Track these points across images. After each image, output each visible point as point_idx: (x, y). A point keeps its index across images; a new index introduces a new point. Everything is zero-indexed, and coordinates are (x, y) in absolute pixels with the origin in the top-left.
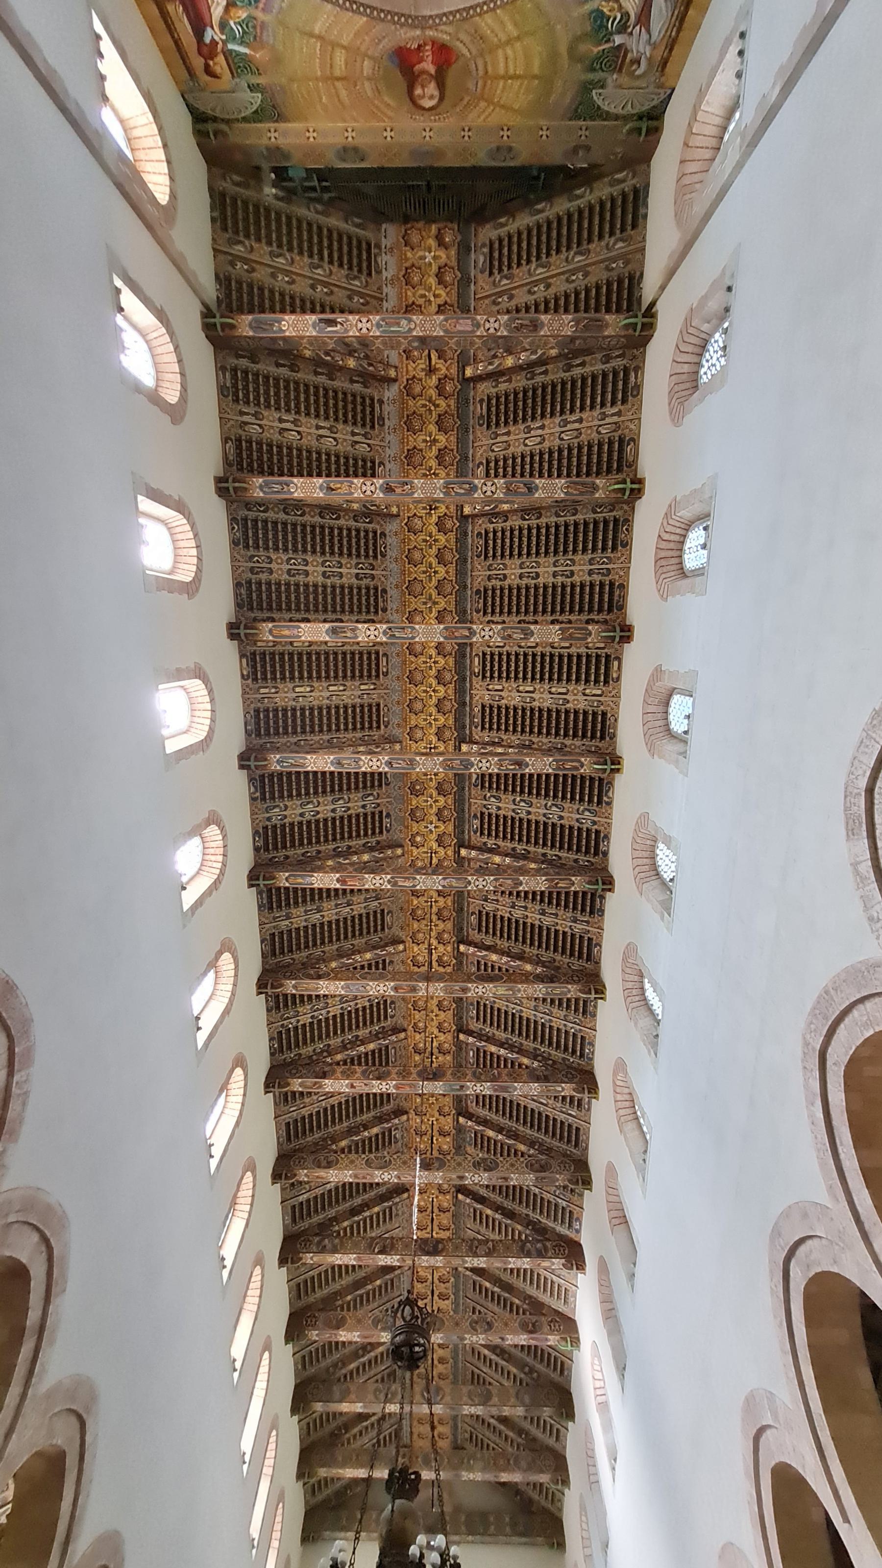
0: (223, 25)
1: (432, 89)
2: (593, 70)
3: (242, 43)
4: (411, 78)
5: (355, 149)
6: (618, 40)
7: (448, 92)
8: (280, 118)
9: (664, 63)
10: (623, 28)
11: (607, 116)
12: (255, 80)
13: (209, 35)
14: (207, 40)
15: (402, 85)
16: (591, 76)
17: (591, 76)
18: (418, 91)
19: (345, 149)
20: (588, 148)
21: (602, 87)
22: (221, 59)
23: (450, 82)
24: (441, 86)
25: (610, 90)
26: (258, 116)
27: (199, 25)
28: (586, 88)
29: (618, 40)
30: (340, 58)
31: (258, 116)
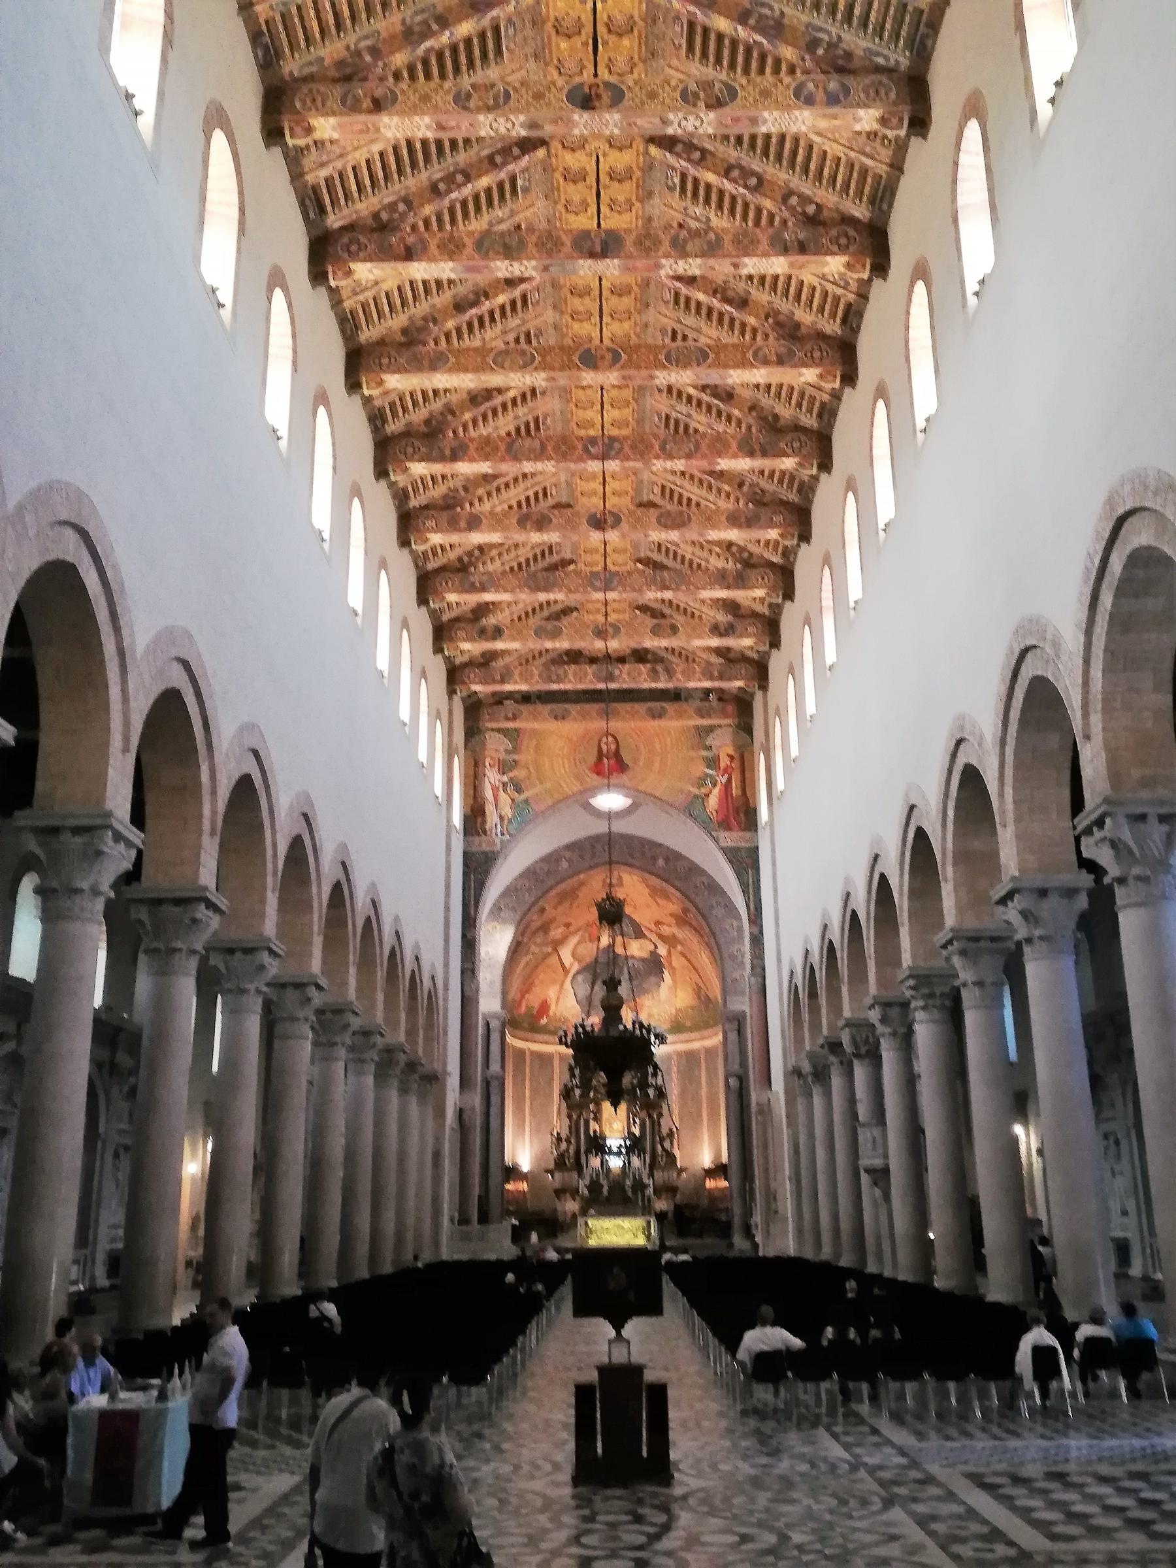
0: (714, 785)
1: (604, 747)
2: (515, 761)
3: (707, 775)
4: (617, 755)
5: (654, 717)
6: (505, 778)
7: (596, 743)
8: (697, 728)
9: (476, 765)
10: (505, 785)
11: (499, 730)
12: (705, 753)
13: (724, 780)
14: (726, 776)
15: (623, 753)
16: (516, 757)
17: (516, 757)
18: (613, 747)
19: (660, 717)
20: (507, 719)
21: (506, 751)
22: (722, 765)
23: (595, 752)
24: (600, 751)
25: (502, 749)
26: (710, 729)
27: (728, 784)
28: (516, 750)
29: (505, 778)
30: (657, 765)
31: (710, 729)
